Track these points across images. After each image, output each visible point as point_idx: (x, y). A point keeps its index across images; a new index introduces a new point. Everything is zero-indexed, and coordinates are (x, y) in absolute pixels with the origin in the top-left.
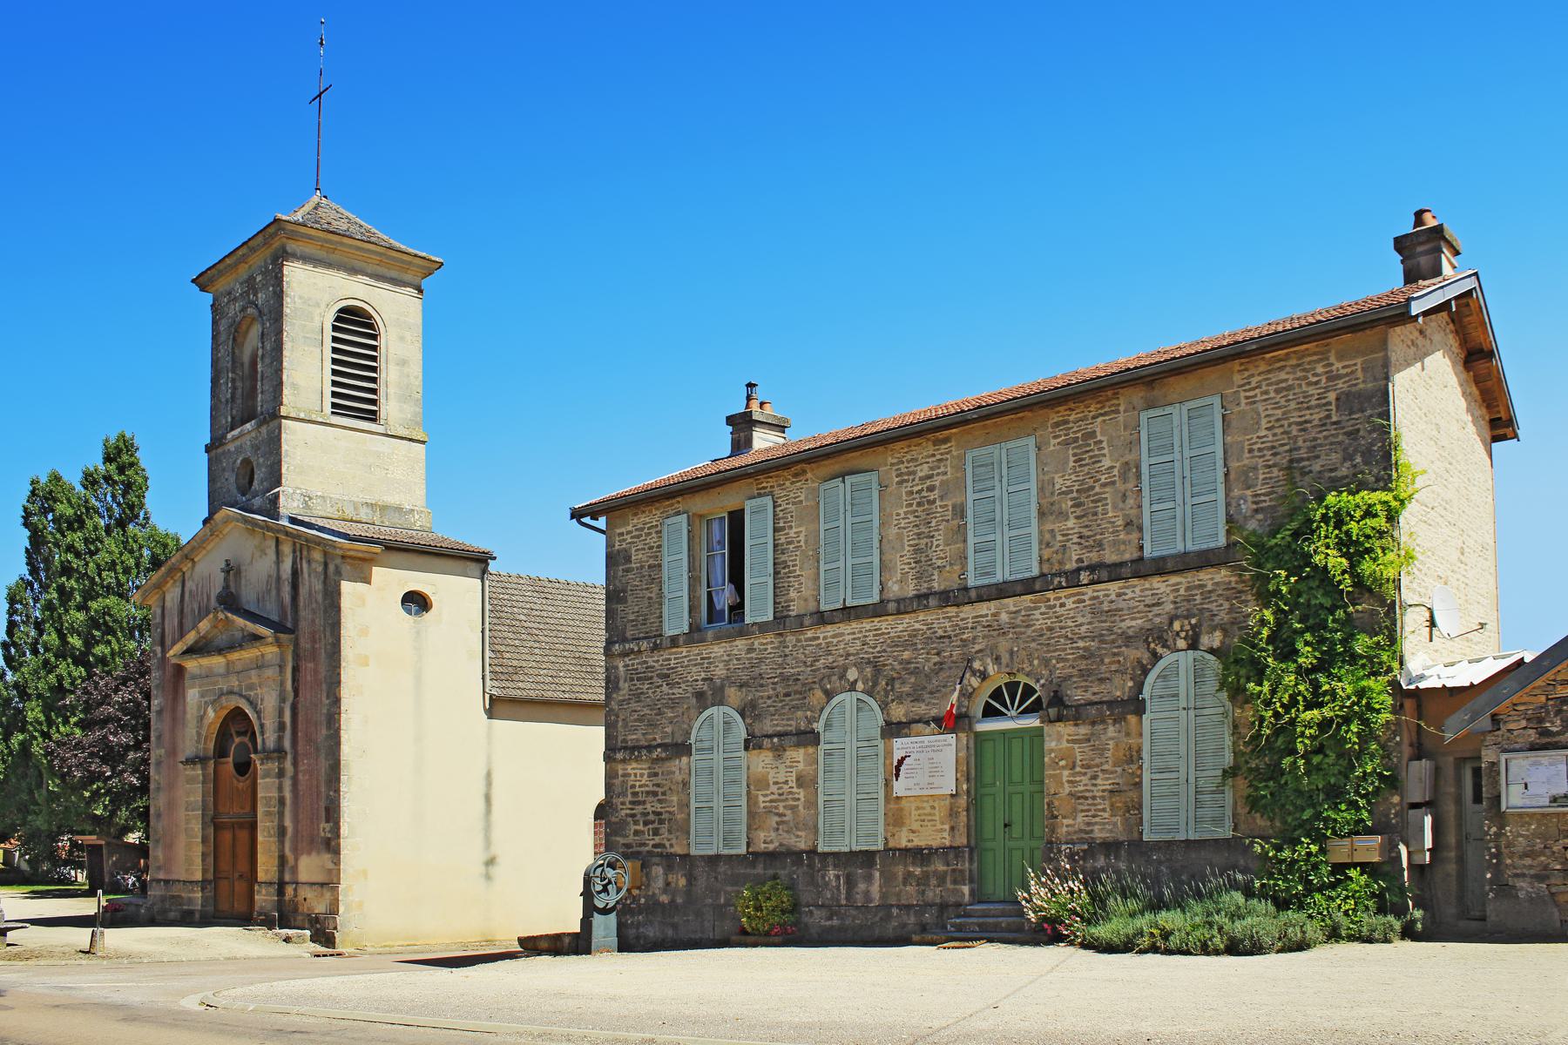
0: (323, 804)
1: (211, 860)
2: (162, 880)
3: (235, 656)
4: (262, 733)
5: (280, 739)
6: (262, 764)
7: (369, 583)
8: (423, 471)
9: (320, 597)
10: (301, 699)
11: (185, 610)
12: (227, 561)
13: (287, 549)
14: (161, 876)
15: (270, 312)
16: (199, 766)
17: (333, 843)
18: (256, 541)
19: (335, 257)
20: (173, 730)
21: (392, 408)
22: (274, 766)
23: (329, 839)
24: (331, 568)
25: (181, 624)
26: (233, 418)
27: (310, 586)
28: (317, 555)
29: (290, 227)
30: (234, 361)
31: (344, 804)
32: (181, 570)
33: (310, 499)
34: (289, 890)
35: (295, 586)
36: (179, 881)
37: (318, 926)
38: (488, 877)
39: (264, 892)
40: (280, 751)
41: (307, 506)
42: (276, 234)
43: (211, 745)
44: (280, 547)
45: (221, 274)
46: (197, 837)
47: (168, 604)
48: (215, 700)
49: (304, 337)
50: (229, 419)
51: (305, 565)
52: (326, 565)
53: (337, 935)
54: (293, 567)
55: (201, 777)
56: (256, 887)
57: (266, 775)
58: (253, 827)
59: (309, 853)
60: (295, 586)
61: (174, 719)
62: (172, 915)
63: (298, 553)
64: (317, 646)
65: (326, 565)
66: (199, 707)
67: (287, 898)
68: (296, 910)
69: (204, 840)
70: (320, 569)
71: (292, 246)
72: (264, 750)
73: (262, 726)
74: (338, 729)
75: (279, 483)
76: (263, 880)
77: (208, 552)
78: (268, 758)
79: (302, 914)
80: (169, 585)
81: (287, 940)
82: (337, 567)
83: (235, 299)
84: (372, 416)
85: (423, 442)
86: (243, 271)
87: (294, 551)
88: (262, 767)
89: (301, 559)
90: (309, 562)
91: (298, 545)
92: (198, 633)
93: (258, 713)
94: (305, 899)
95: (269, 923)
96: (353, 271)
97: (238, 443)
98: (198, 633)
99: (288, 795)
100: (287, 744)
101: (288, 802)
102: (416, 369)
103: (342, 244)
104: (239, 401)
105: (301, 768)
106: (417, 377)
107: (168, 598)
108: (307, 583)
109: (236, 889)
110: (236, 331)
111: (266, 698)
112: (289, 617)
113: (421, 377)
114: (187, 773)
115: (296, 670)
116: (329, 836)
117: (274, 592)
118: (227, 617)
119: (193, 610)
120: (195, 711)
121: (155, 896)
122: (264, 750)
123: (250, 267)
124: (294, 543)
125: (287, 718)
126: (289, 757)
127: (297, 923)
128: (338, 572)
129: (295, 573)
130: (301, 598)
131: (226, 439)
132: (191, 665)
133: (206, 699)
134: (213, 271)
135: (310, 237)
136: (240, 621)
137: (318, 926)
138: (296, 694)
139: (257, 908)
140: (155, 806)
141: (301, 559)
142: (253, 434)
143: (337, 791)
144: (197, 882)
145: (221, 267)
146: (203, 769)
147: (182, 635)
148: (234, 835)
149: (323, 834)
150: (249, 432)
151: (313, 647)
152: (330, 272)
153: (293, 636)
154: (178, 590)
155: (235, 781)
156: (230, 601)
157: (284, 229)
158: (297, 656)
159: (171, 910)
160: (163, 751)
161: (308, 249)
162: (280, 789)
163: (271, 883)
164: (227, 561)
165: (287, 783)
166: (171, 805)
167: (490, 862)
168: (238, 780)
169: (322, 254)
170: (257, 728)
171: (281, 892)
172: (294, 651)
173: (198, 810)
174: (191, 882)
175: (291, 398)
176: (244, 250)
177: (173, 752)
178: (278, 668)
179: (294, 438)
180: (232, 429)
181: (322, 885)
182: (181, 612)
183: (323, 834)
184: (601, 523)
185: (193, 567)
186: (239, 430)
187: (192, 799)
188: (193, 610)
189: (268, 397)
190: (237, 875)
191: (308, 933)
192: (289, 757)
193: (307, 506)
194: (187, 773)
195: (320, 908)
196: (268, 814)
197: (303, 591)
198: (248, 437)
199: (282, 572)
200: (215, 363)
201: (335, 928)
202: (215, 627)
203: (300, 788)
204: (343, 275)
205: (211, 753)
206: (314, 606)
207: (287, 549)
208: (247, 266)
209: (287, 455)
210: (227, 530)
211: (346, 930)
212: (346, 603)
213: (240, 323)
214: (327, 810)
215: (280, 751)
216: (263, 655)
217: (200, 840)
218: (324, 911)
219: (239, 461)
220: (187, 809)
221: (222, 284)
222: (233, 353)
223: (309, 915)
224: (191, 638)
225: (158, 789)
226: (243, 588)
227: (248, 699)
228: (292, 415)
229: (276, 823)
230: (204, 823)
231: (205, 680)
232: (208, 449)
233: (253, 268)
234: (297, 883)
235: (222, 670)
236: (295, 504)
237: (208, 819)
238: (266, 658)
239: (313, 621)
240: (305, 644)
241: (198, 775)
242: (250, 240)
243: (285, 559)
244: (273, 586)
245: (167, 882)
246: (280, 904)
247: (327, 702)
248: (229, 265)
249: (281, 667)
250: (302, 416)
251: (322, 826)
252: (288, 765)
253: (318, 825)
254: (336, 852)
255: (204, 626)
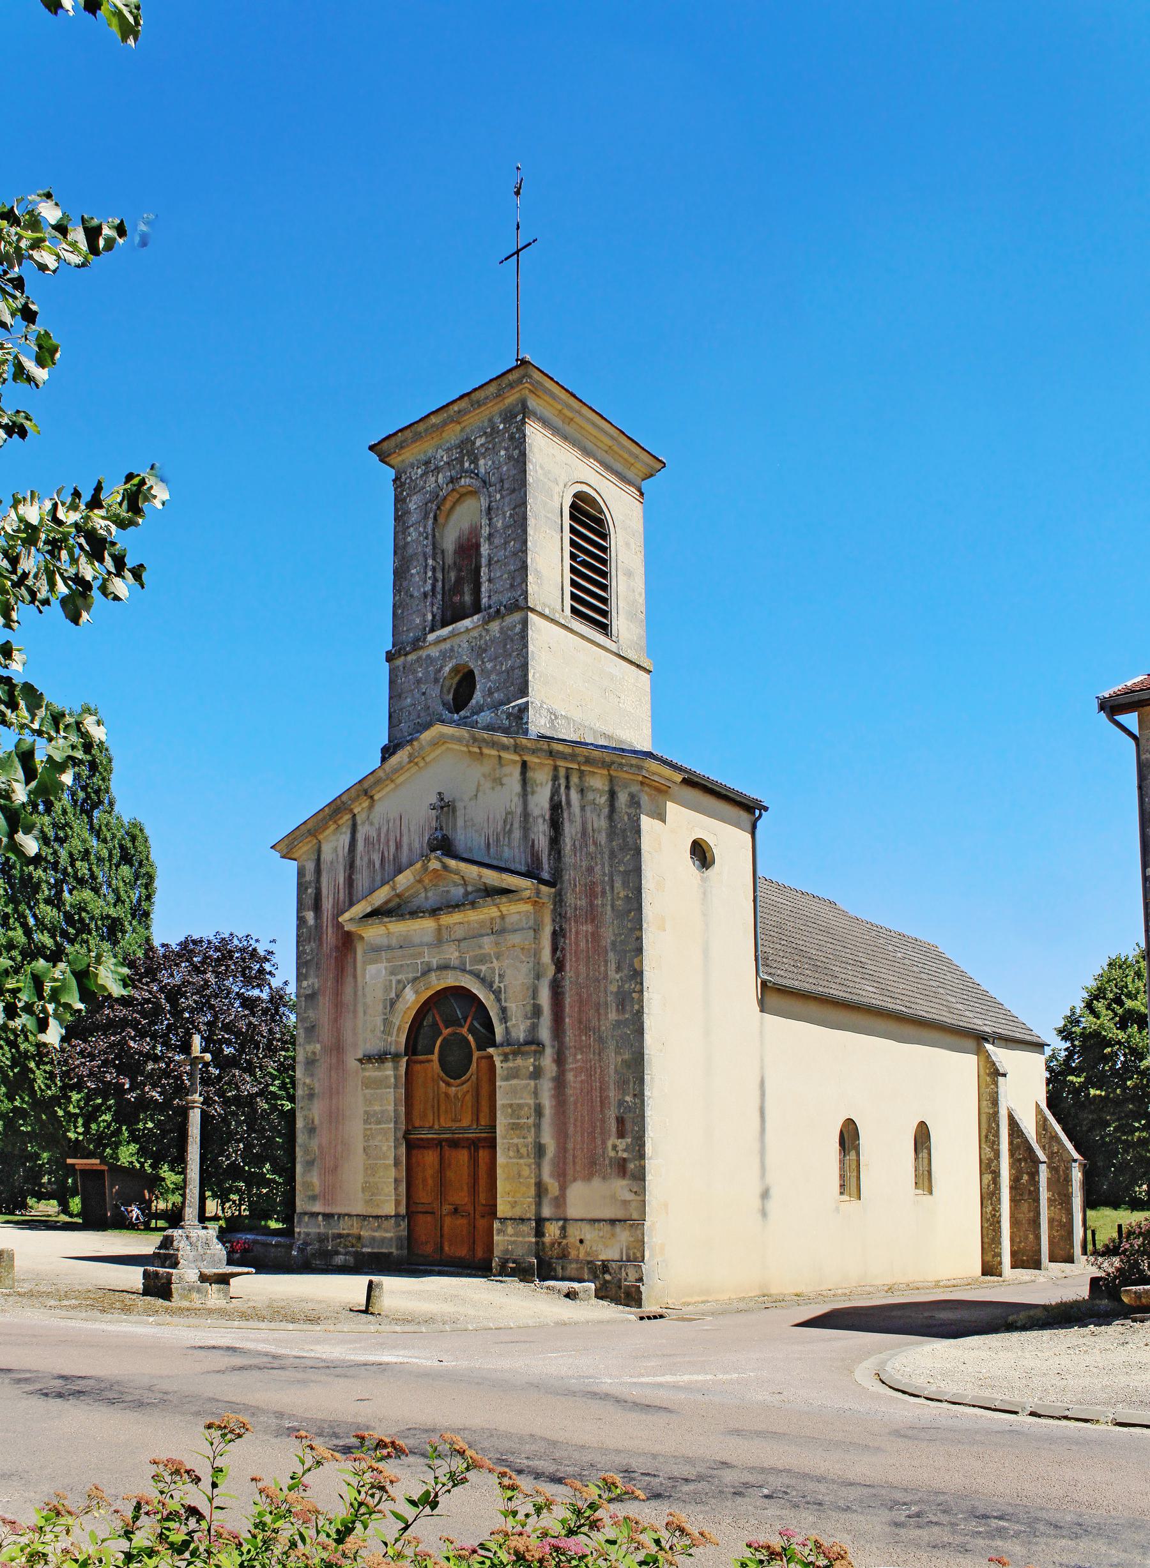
0: (612, 1113)
1: (403, 1188)
2: (318, 1214)
3: (447, 919)
4: (504, 1019)
5: (534, 1028)
6: (506, 1059)
7: (664, 821)
8: (649, 706)
9: (602, 838)
10: (569, 973)
11: (358, 862)
12: (440, 794)
13: (542, 777)
14: (317, 1208)
15: (502, 481)
16: (389, 1065)
17: (631, 1166)
18: (486, 767)
19: (569, 430)
20: (336, 1019)
21: (620, 622)
22: (526, 1063)
23: (624, 1160)
24: (622, 798)
25: (350, 882)
26: (434, 616)
27: (584, 824)
28: (598, 782)
29: (537, 376)
30: (434, 547)
31: (648, 1113)
32: (351, 811)
33: (556, 718)
34: (552, 1231)
35: (556, 824)
36: (349, 1215)
37: (608, 1277)
38: (764, 1213)
39: (510, 1230)
40: (533, 1042)
41: (553, 727)
42: (519, 381)
43: (403, 1039)
44: (530, 774)
45: (417, 437)
46: (385, 1158)
47: (327, 854)
48: (415, 979)
49: (545, 516)
50: (429, 617)
51: (574, 796)
52: (612, 795)
53: (643, 1289)
54: (552, 799)
55: (393, 1080)
56: (496, 1225)
57: (513, 1074)
58: (492, 1144)
59: (588, 1178)
60: (556, 824)
61: (338, 1005)
62: (339, 1260)
63: (562, 781)
64: (599, 902)
65: (612, 795)
66: (387, 989)
67: (547, 1239)
68: (564, 1256)
69: (397, 1164)
70: (603, 800)
71: (532, 403)
72: (508, 1042)
73: (504, 1010)
74: (640, 1014)
75: (524, 691)
76: (509, 1215)
77: (397, 786)
78: (515, 1054)
79: (577, 1261)
80: (327, 832)
81: (570, 1295)
82: (632, 796)
83: (438, 469)
84: (604, 628)
85: (649, 672)
86: (453, 434)
87: (555, 778)
88: (505, 1065)
89: (568, 787)
90: (582, 791)
91: (562, 772)
92: (394, 889)
93: (497, 993)
94: (581, 1241)
95: (523, 1273)
96: (587, 452)
97: (446, 646)
98: (394, 889)
99: (547, 1103)
100: (545, 1034)
101: (548, 1111)
102: (639, 583)
103: (579, 413)
104: (439, 597)
105: (570, 1065)
106: (640, 594)
107: (327, 849)
108: (578, 819)
109: (446, 1228)
110: (439, 508)
111: (508, 972)
112: (546, 866)
113: (644, 595)
114: (367, 1074)
115: (557, 935)
116: (625, 1155)
117: (517, 834)
118: (445, 867)
119: (371, 863)
120: (380, 994)
121: (308, 1234)
122: (508, 1042)
123: (462, 430)
124: (556, 768)
125: (545, 998)
126: (549, 1051)
127: (568, 1273)
128: (635, 802)
129: (556, 808)
130: (568, 840)
131: (424, 641)
132: (374, 933)
133: (399, 977)
134: (408, 433)
135: (554, 396)
136: (472, 871)
137: (608, 1277)
138: (560, 966)
139: (497, 1252)
140: (305, 1118)
141: (568, 787)
142: (475, 633)
143: (640, 1095)
144: (387, 1217)
145: (421, 427)
146: (396, 1069)
147: (372, 891)
148: (442, 1158)
149: (612, 1154)
150: (468, 630)
151: (591, 904)
152: (566, 446)
153: (553, 890)
154: (345, 839)
155: (442, 1085)
156: (444, 845)
157: (530, 377)
158: (559, 915)
159: (337, 1253)
160: (318, 1046)
161: (548, 413)
162: (536, 1094)
163: (522, 1220)
164: (440, 794)
165: (546, 1087)
166: (335, 1117)
167: (765, 1195)
168: (448, 1084)
169: (558, 422)
170: (494, 1014)
171: (539, 1233)
172: (554, 910)
173: (388, 1122)
174: (377, 1217)
175: (536, 588)
176: (463, 404)
177: (337, 1048)
178: (531, 933)
179: (541, 634)
180: (432, 630)
181: (613, 1222)
182: (351, 865)
183: (612, 1154)
184: (1130, 720)
185: (371, 807)
186: (450, 628)
187: (377, 1108)
188: (371, 863)
189: (503, 584)
190: (447, 1208)
191: (592, 1286)
192: (549, 1051)
193: (553, 727)
194: (367, 1074)
195: (609, 1252)
196: (515, 1127)
197: (570, 831)
198: (465, 638)
199: (531, 806)
200: (399, 549)
201: (641, 1280)
202: (420, 881)
203: (569, 1091)
204: (578, 454)
205: (402, 1048)
206: (592, 849)
207: (542, 777)
208: (458, 428)
209: (533, 659)
210: (432, 756)
211: (651, 1283)
212: (647, 844)
213: (445, 498)
214: (620, 1121)
215: (533, 1042)
216: (503, 917)
217: (391, 1162)
218: (617, 1257)
219: (447, 669)
220: (366, 1122)
221: (410, 455)
222: (434, 536)
223: (589, 1262)
224: (381, 896)
225: (311, 1096)
226: (460, 831)
227: (476, 975)
228: (539, 608)
229: (530, 1139)
230: (396, 1139)
231: (399, 952)
232: (390, 657)
233: (468, 430)
234: (565, 1220)
235: (429, 938)
236: (542, 722)
237: (400, 1134)
238: (507, 920)
239: (590, 870)
240: (574, 900)
241: (387, 1077)
242: (475, 390)
243: (538, 789)
244: (516, 825)
245: (328, 1216)
246: (539, 1250)
247: (618, 977)
248: (433, 426)
249: (536, 930)
250: (547, 612)
251: (610, 1144)
252: (547, 1061)
253: (604, 1143)
254: (640, 1177)
255: (404, 880)
